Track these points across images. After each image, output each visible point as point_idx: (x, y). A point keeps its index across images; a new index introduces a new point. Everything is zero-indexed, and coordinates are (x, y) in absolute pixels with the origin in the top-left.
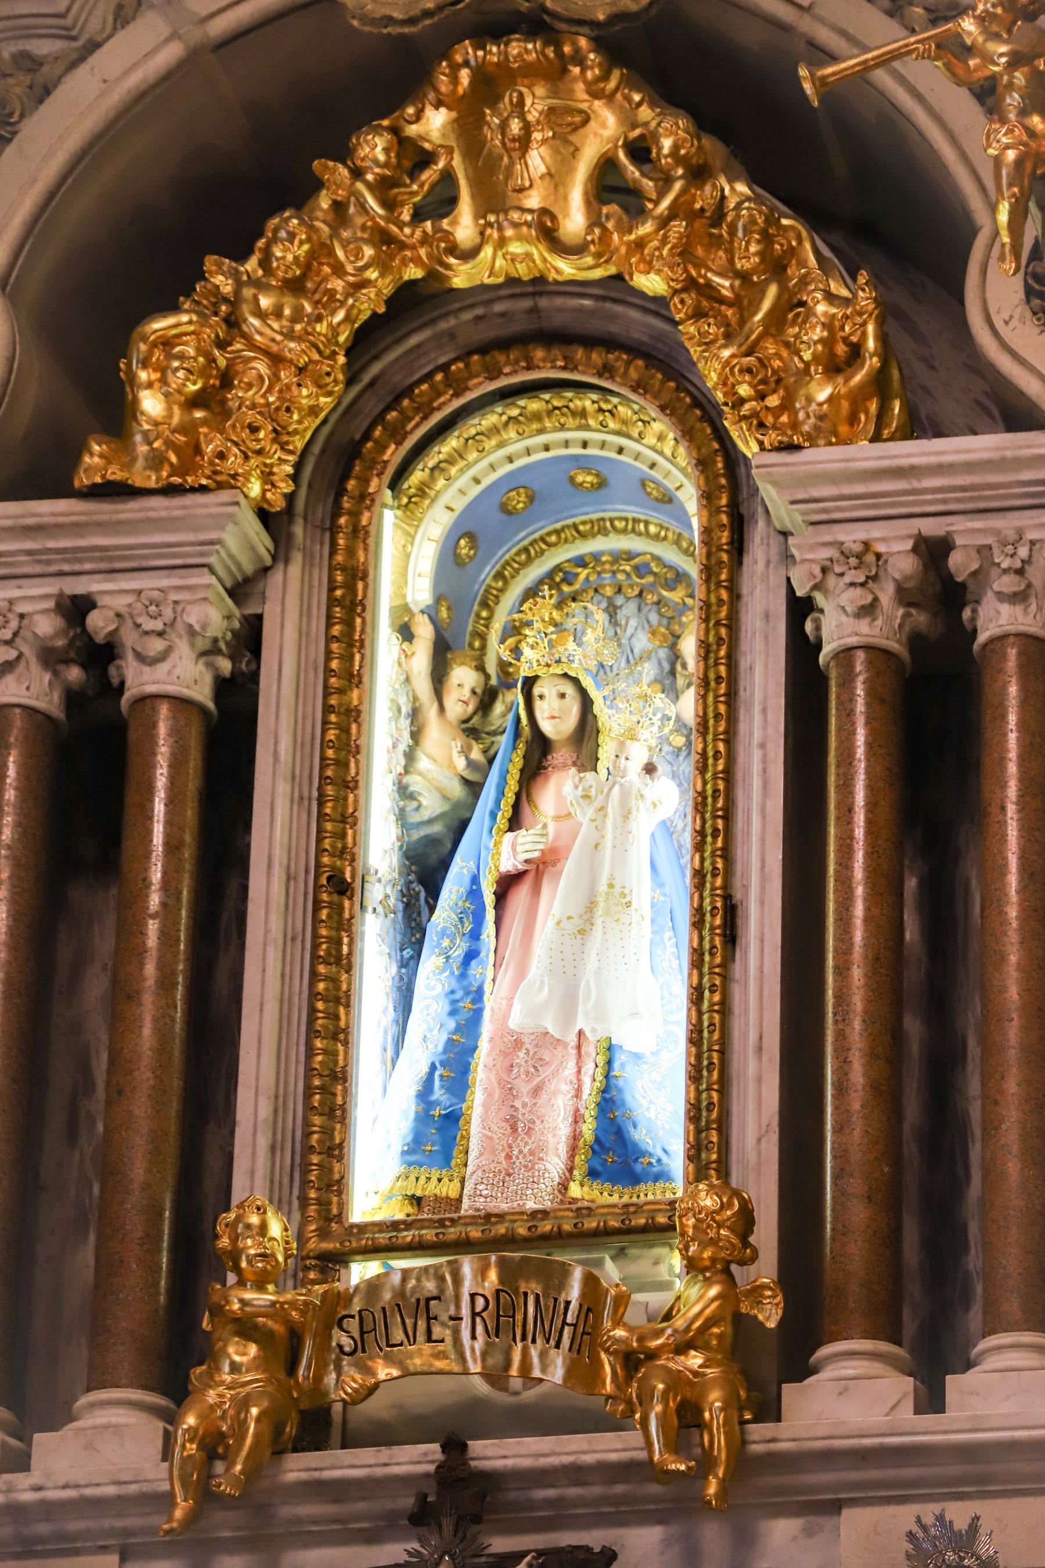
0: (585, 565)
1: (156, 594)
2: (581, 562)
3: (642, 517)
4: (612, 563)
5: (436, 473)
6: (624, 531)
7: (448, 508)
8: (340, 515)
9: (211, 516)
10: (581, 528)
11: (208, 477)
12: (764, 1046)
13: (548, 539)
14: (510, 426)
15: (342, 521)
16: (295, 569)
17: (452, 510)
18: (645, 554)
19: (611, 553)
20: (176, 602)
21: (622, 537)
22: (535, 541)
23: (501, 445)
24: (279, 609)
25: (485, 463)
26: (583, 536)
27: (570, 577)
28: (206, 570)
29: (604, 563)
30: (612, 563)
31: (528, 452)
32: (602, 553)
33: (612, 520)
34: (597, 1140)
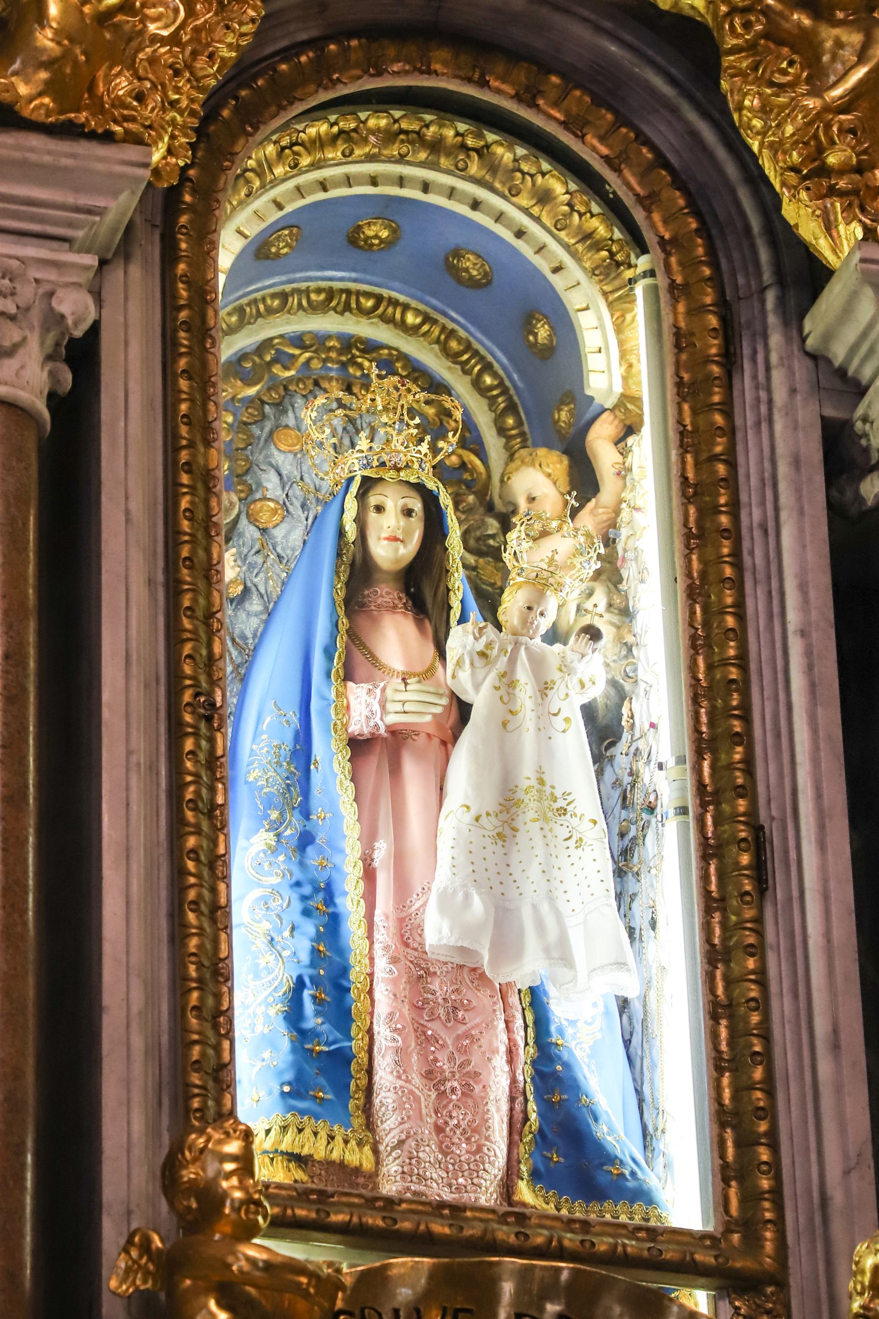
0: (304, 348)
1: (15, 263)
2: (299, 341)
3: (402, 298)
4: (340, 352)
5: (241, 182)
6: (367, 313)
7: (239, 232)
8: (183, 212)
9: (111, 175)
10: (313, 296)
11: (116, 122)
12: (843, 1043)
13: (269, 302)
14: (339, 142)
15: (184, 219)
16: (135, 270)
17: (246, 237)
18: (390, 348)
19: (340, 337)
20: (37, 281)
21: (364, 320)
22: (255, 301)
23: (315, 166)
24: (122, 320)
25: (291, 184)
26: (314, 308)
27: (284, 358)
28: (66, 246)
29: (330, 349)
30: (340, 352)
31: (348, 181)
32: (329, 337)
33: (358, 293)
34: (541, 1131)
